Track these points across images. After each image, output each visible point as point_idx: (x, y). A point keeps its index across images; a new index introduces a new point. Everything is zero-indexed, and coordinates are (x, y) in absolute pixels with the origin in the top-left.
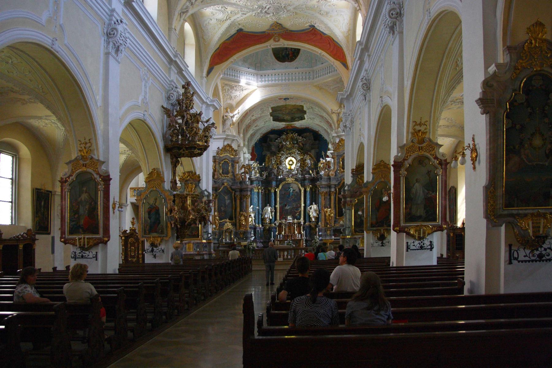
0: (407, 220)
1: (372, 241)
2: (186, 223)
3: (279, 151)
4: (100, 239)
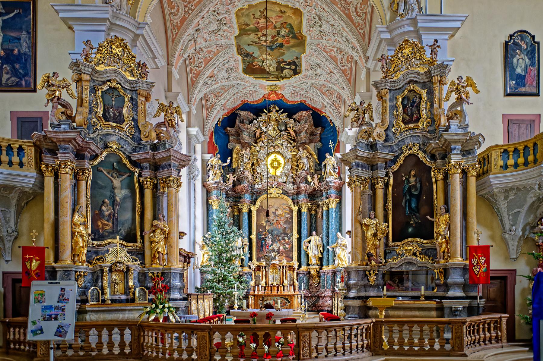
3: (256, 143)
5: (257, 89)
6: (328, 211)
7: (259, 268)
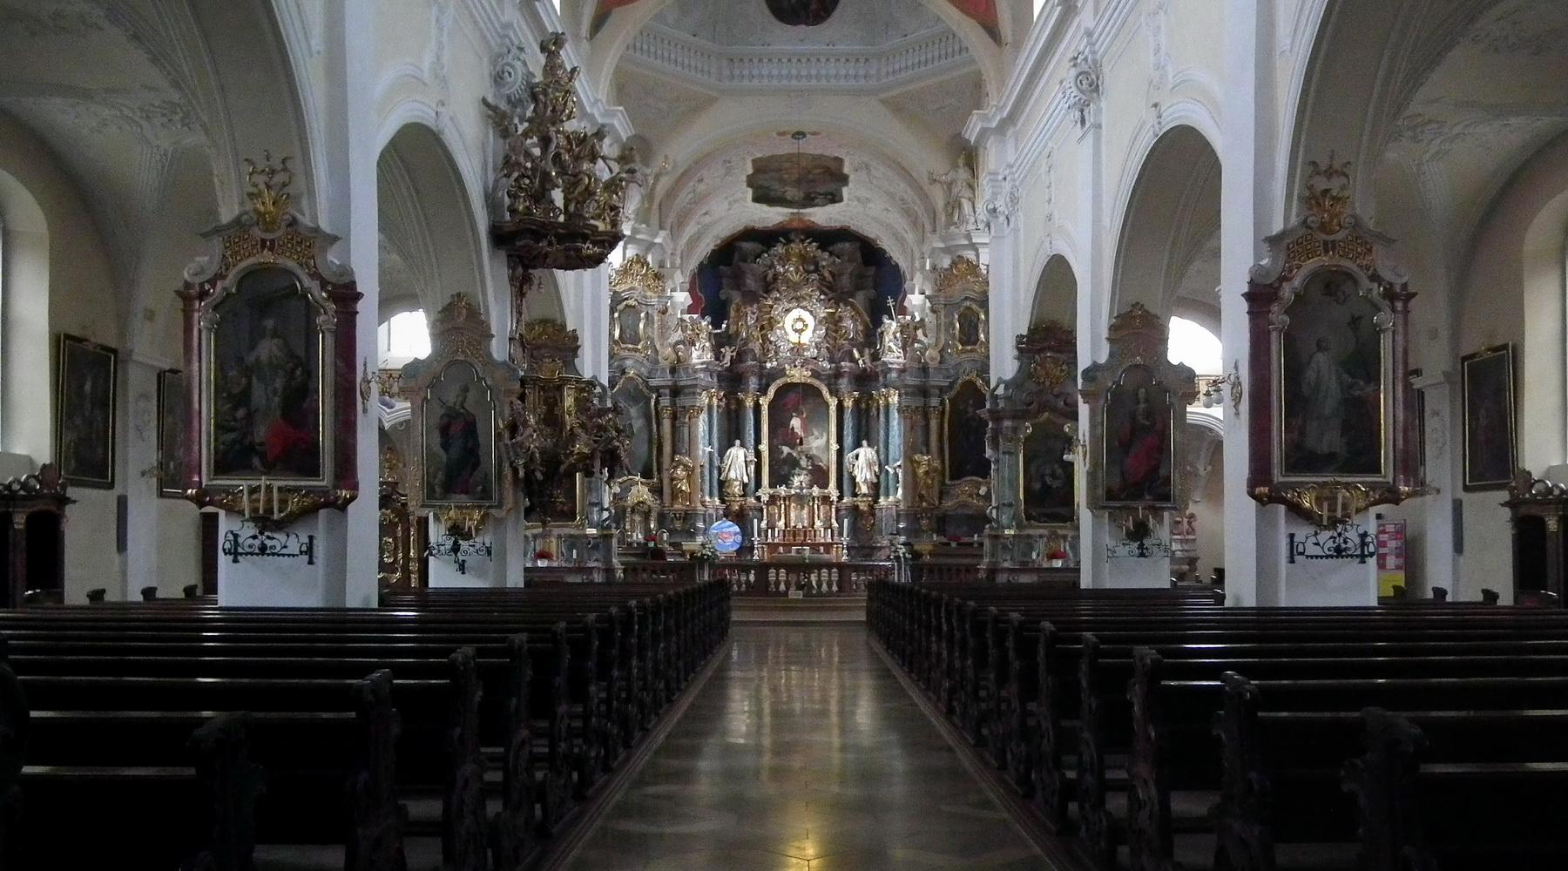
0: (1292, 467)
1: (1108, 541)
3: (768, 291)
4: (324, 492)
5: (772, 216)
6: (887, 406)
7: (773, 499)
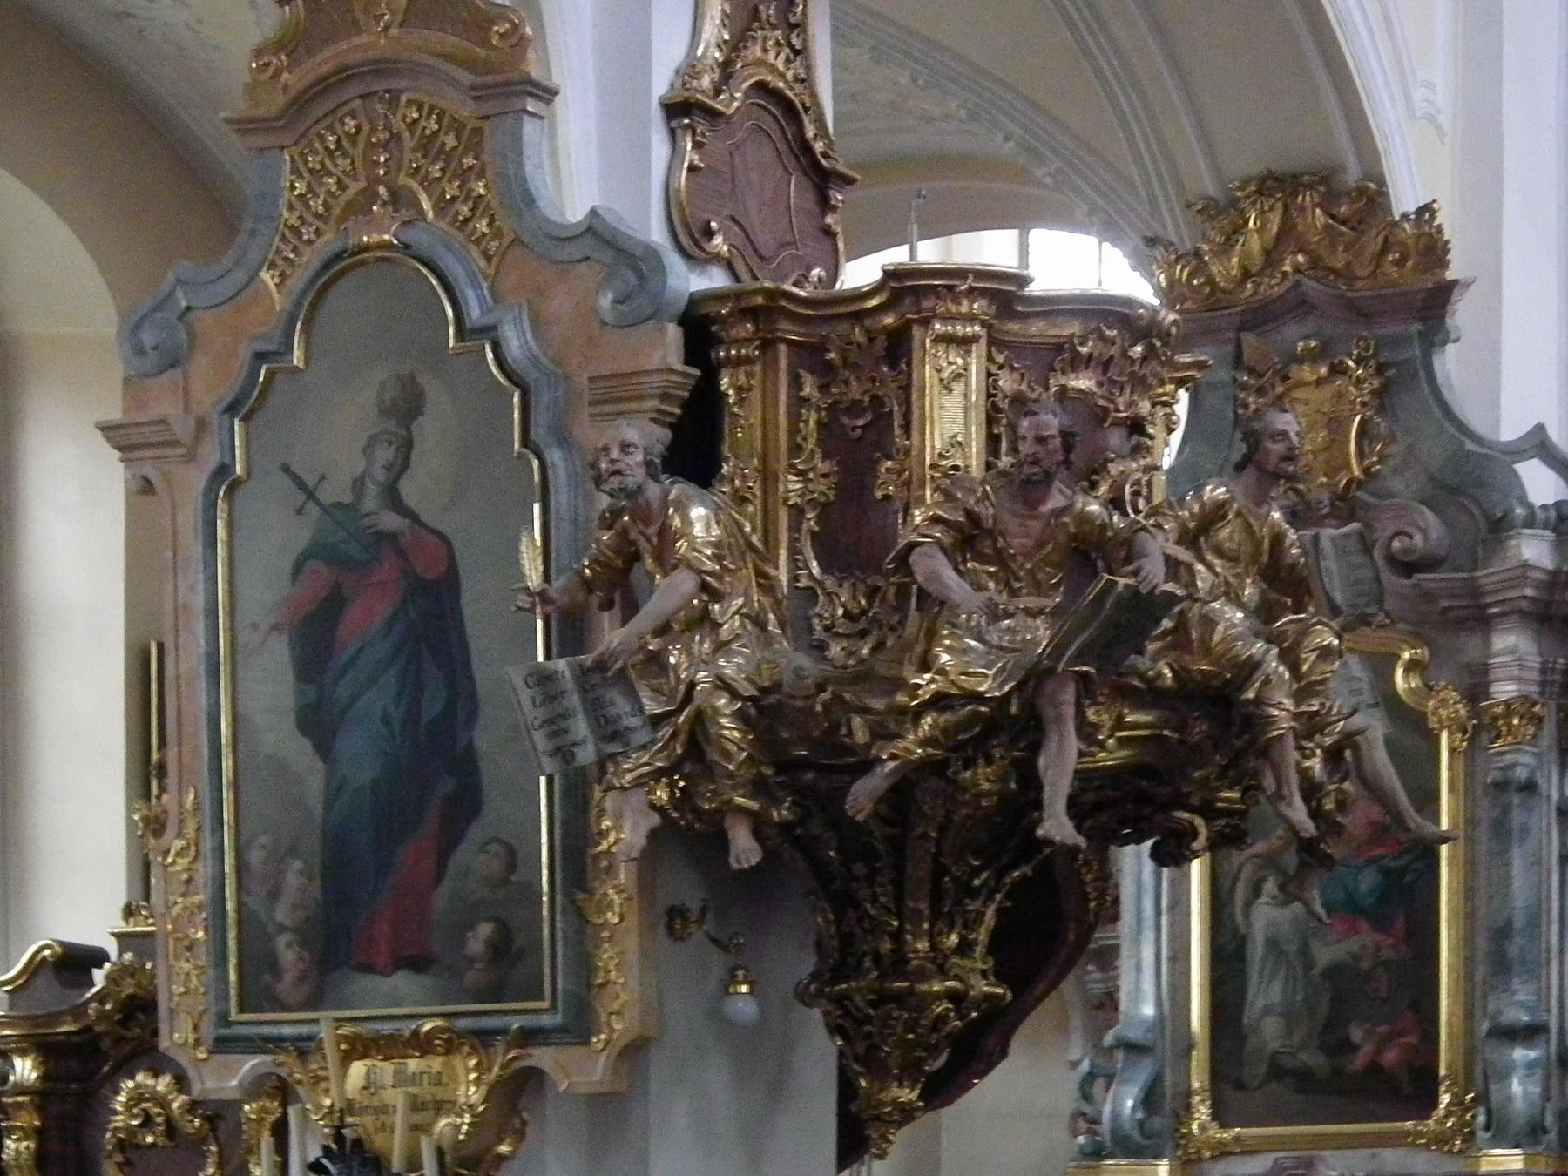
2: (863, 796)
